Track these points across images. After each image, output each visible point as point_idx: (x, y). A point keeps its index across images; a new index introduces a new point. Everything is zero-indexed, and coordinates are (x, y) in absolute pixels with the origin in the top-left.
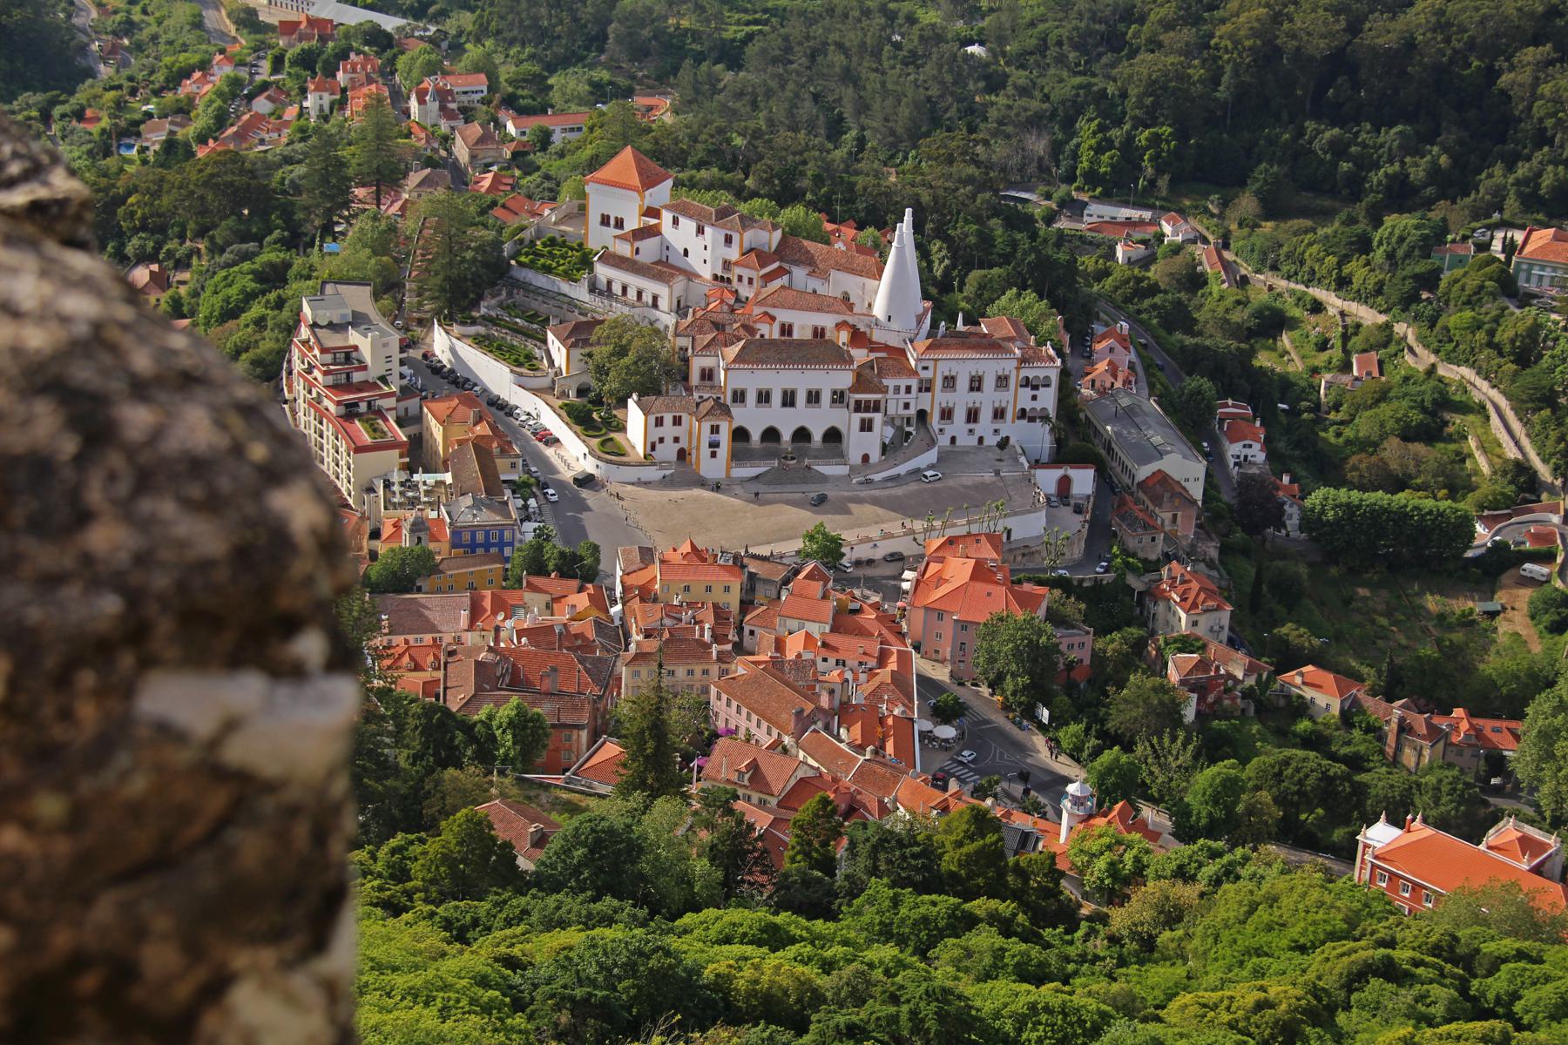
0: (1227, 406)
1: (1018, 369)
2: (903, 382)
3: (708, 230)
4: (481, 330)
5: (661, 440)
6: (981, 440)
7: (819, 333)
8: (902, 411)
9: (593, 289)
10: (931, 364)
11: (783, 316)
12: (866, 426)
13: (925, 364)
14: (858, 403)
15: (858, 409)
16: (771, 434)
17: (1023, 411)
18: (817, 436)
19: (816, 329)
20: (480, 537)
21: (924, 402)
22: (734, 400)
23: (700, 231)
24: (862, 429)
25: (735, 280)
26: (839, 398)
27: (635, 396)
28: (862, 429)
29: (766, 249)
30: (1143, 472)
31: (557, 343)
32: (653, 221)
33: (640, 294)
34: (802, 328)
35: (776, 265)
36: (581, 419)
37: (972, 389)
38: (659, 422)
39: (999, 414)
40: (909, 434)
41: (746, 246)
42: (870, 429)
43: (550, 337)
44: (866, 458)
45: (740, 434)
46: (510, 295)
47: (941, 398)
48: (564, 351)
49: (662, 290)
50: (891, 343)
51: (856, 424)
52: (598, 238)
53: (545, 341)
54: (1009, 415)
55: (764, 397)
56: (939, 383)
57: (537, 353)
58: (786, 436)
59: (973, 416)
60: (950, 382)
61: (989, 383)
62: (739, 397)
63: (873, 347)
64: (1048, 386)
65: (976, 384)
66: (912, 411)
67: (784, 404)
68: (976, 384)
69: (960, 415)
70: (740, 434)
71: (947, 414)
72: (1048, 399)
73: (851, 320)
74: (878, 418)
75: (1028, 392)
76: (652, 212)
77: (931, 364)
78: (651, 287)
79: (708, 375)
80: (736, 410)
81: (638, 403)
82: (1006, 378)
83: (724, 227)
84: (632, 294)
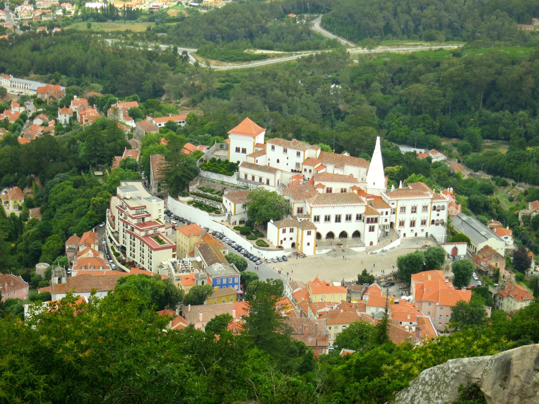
0: (491, 222)
1: (431, 203)
2: (384, 210)
3: (288, 150)
4: (190, 198)
5: (285, 239)
6: (416, 234)
7: (343, 191)
9: (239, 179)
10: (395, 202)
11: (328, 185)
12: (372, 229)
13: (393, 202)
14: (368, 219)
16: (330, 235)
18: (350, 234)
19: (342, 189)
20: (225, 282)
22: (315, 220)
23: (285, 151)
24: (370, 231)
25: (303, 170)
26: (359, 217)
27: (272, 221)
28: (370, 231)
29: (315, 157)
30: (480, 246)
31: (229, 201)
32: (260, 149)
33: (261, 179)
34: (336, 189)
35: (320, 164)
36: (244, 233)
37: (412, 212)
38: (284, 231)
39: (424, 223)
40: (387, 233)
41: (306, 158)
43: (224, 199)
44: (371, 243)
45: (318, 236)
46: (201, 182)
47: (400, 216)
48: (233, 204)
49: (270, 176)
50: (375, 194)
51: (367, 228)
52: (234, 157)
53: (222, 202)
54: (428, 223)
55: (327, 219)
57: (219, 207)
58: (337, 235)
59: (413, 224)
61: (419, 209)
62: (317, 219)
63: (368, 196)
64: (443, 209)
65: (414, 210)
66: (388, 223)
67: (336, 221)
68: (414, 210)
69: (407, 224)
70: (318, 236)
71: (402, 224)
73: (357, 185)
74: (376, 225)
75: (435, 212)
76: (258, 145)
77: (395, 202)
78: (265, 176)
79: (300, 211)
80: (316, 224)
81: (273, 224)
82: (426, 207)
83: (295, 149)
84: (257, 180)
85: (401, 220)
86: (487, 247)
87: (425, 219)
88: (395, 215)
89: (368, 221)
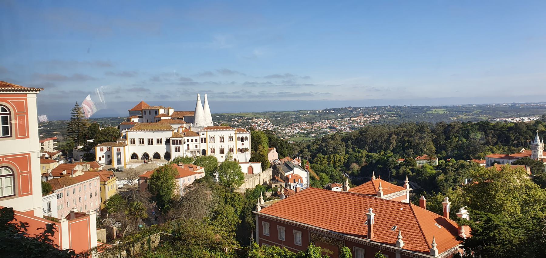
2: (194, 138)
8: (195, 149)
10: (205, 133)
13: (203, 133)
14: (173, 141)
15: (173, 144)
16: (146, 156)
17: (239, 149)
24: (176, 151)
42: (179, 151)
56: (208, 140)
60: (213, 138)
61: (226, 139)
65: (222, 140)
68: (222, 140)
72: (247, 144)
82: (232, 137)
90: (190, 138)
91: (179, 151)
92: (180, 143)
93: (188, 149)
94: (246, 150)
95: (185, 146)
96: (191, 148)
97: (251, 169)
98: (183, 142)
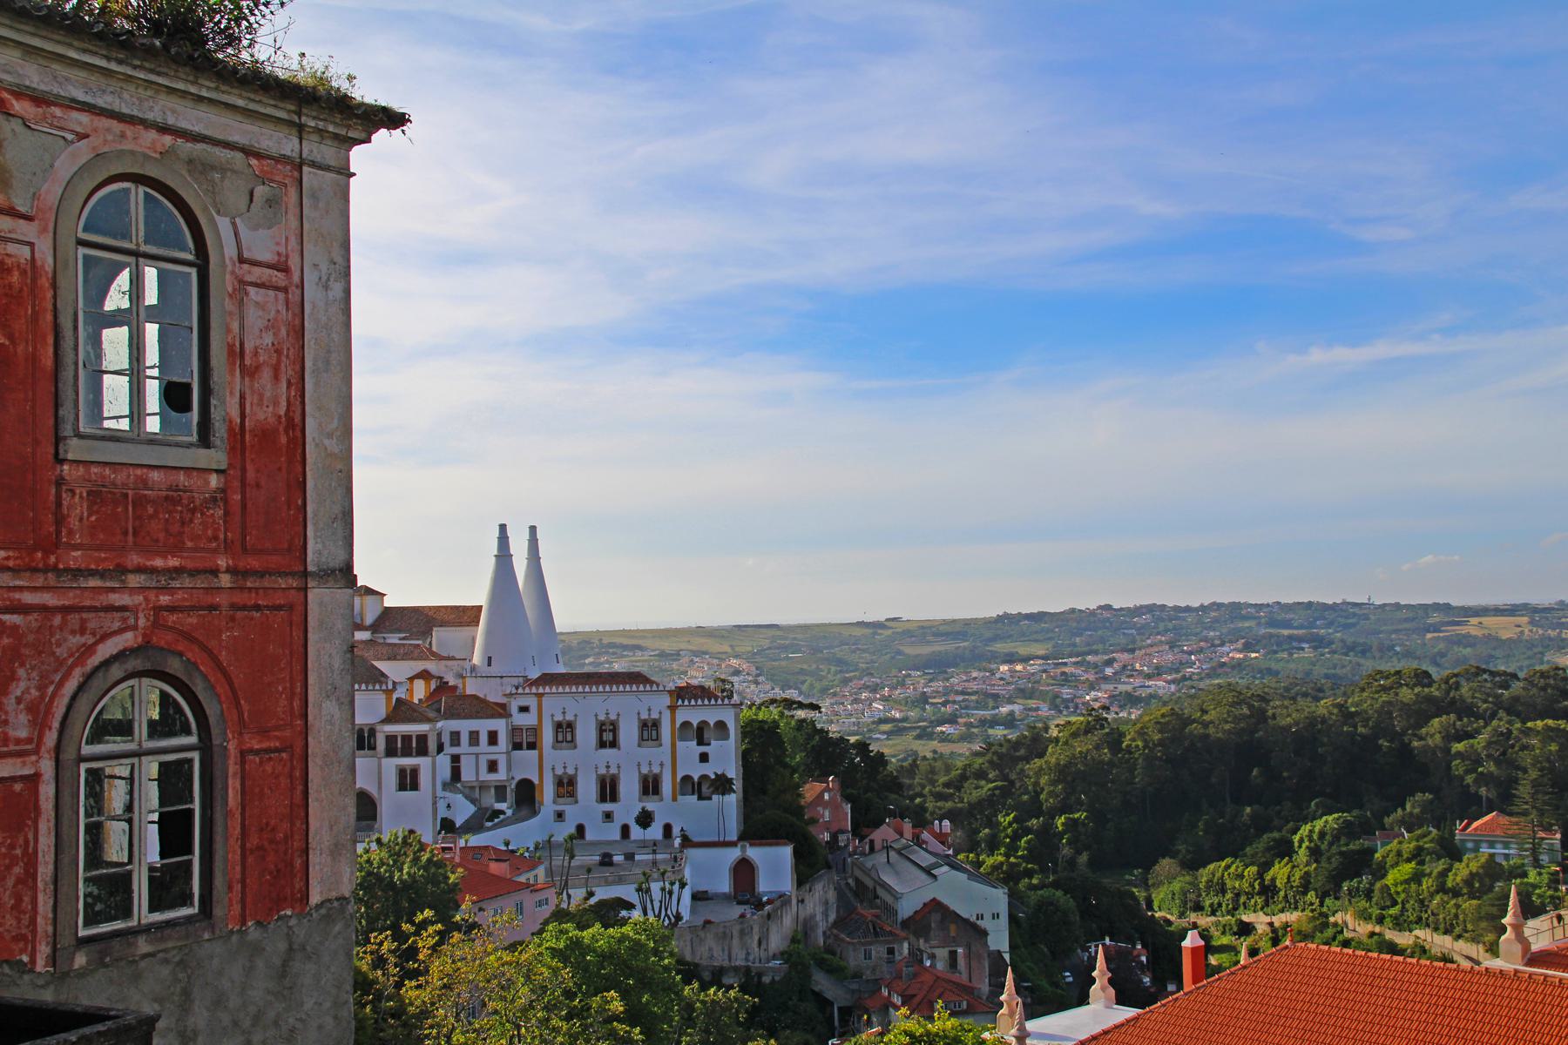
1: (673, 708)
2: (484, 726)
10: (532, 702)
13: (523, 702)
14: (391, 739)
21: (525, 766)
37: (602, 744)
39: (650, 786)
42: (415, 786)
54: (666, 787)
56: (548, 735)
59: (608, 790)
61: (628, 733)
68: (608, 736)
69: (587, 788)
72: (726, 758)
82: (656, 724)
85: (559, 772)
86: (935, 905)
87: (656, 770)
88: (535, 753)
89: (391, 752)
90: (464, 726)
91: (415, 786)
92: (422, 751)
93: (456, 773)
94: (722, 784)
95: (444, 762)
96: (467, 775)
97: (744, 872)
98: (432, 745)
